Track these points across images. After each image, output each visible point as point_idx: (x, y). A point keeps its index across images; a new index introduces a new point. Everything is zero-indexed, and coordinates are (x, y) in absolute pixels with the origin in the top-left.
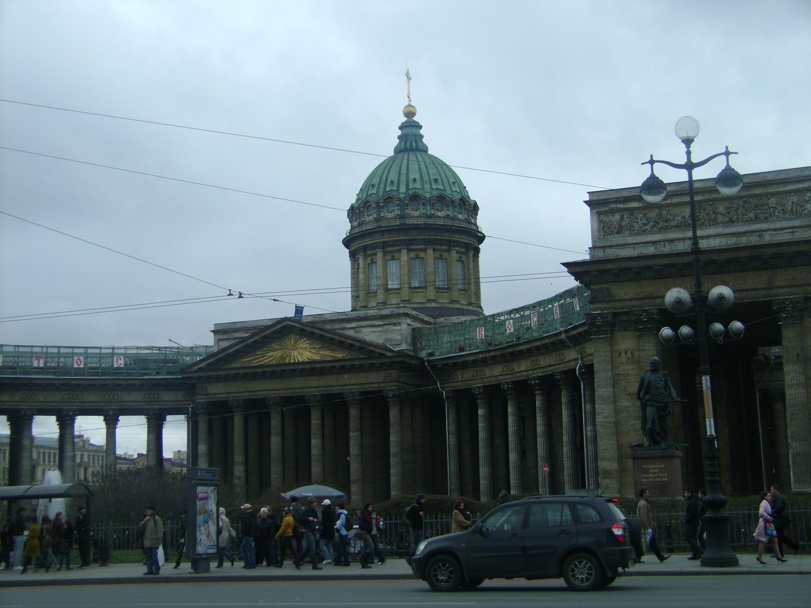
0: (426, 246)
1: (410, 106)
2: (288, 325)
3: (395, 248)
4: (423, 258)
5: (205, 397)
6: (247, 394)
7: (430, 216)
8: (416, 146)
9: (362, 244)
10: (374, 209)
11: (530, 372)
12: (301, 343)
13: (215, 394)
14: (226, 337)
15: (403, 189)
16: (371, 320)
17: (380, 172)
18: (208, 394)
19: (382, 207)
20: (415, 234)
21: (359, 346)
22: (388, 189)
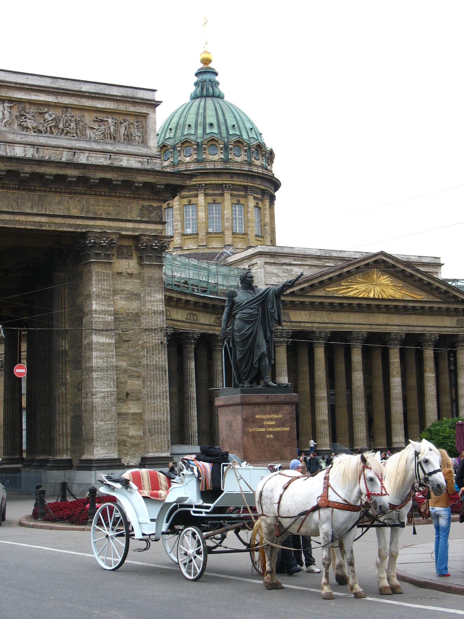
0: (263, 196)
1: (206, 52)
2: (380, 259)
3: (241, 193)
4: (260, 208)
5: (289, 324)
6: (333, 325)
7: (267, 169)
8: (213, 92)
9: (205, 182)
10: (221, 149)
12: (383, 279)
14: (273, 262)
15: (245, 137)
19: (231, 149)
21: (445, 291)
22: (231, 132)
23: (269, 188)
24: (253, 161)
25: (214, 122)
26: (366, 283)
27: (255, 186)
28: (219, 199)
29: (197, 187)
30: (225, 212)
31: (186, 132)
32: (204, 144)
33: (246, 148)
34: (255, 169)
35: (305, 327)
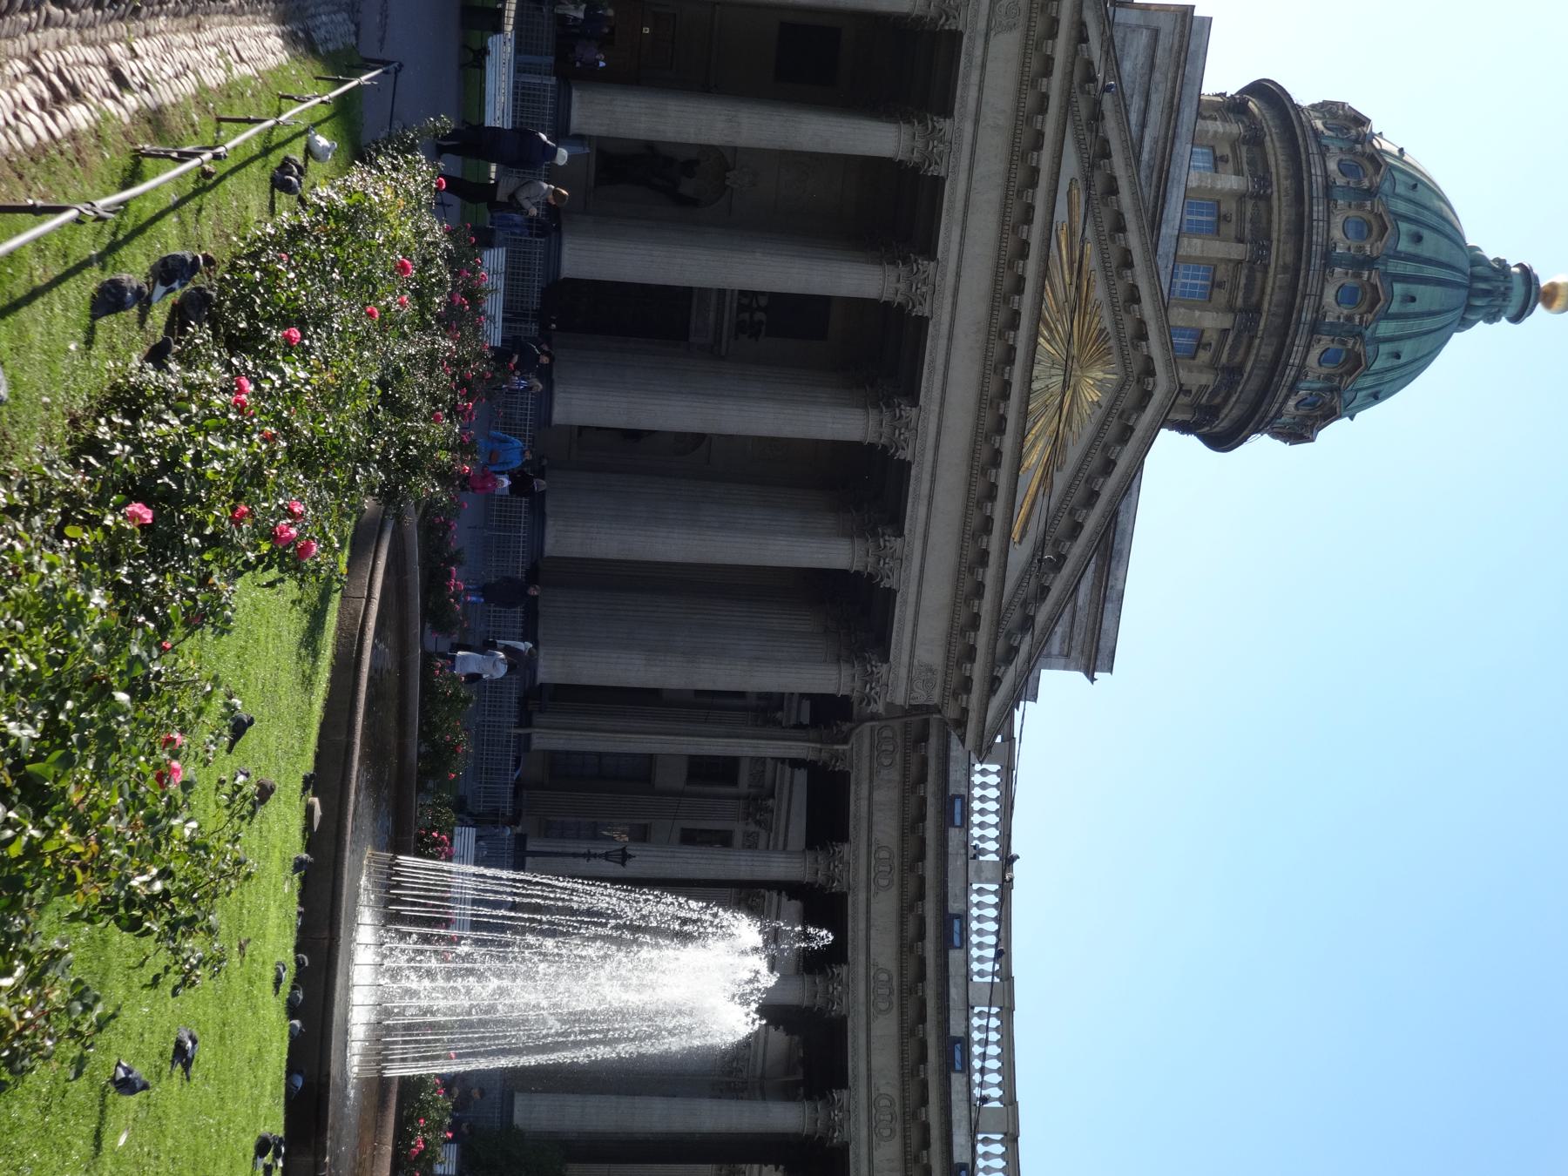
0: (1225, 369)
3: (1241, 294)
4: (1194, 358)
5: (982, 25)
7: (1293, 389)
9: (1275, 195)
10: (1360, 249)
11: (863, 1091)
13: (983, 66)
14: (1158, 61)
15: (1385, 328)
16: (1095, 571)
17: (1444, 251)
18: (987, 35)
19: (1358, 276)
20: (1262, 352)
21: (1033, 618)
23: (1241, 392)
24: (1320, 340)
25: (1427, 249)
26: (1080, 338)
27: (1252, 338)
28: (1230, 229)
29: (1263, 179)
30: (1197, 242)
31: (1397, 175)
32: (1372, 205)
33: (1357, 320)
34: (1300, 341)
35: (966, 86)
